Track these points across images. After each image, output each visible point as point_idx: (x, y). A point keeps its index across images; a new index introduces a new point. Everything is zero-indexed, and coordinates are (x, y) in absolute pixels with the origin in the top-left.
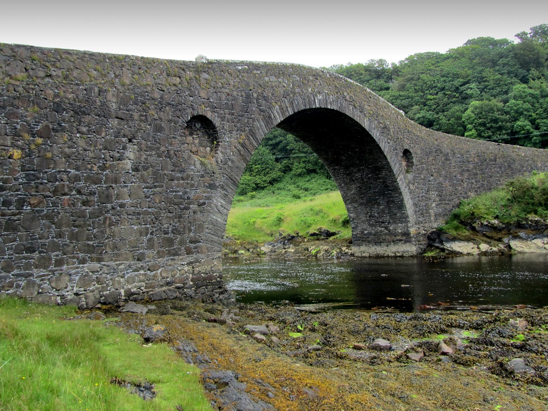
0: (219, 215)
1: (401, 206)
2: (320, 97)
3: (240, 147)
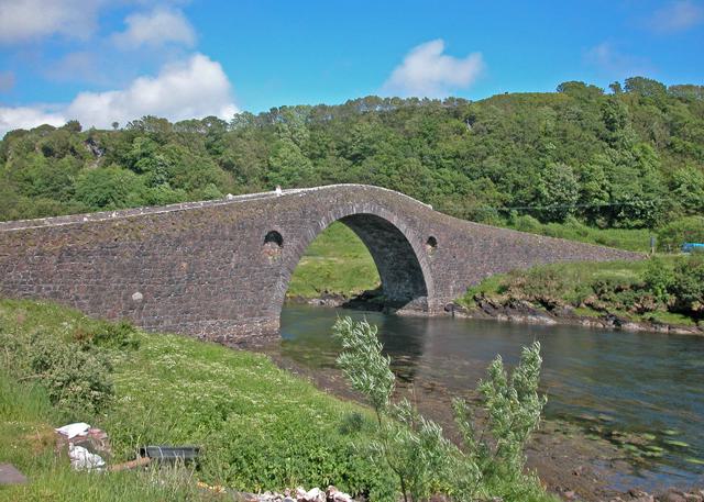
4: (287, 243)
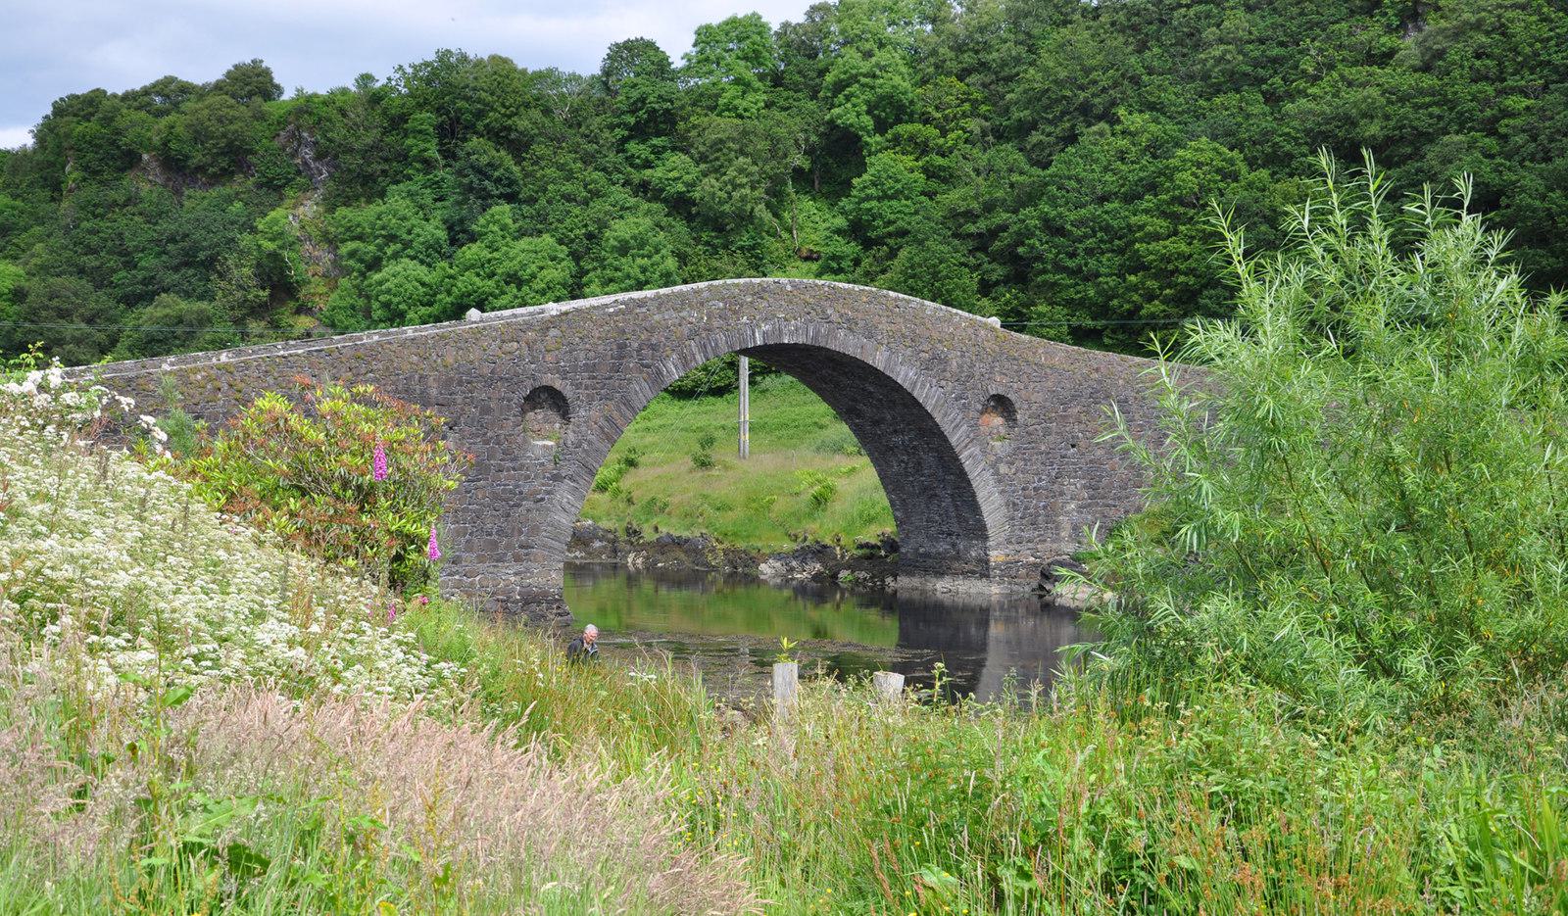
0: (564, 515)
1: (974, 507)
2: (765, 327)
3: (602, 422)
4: (580, 413)
